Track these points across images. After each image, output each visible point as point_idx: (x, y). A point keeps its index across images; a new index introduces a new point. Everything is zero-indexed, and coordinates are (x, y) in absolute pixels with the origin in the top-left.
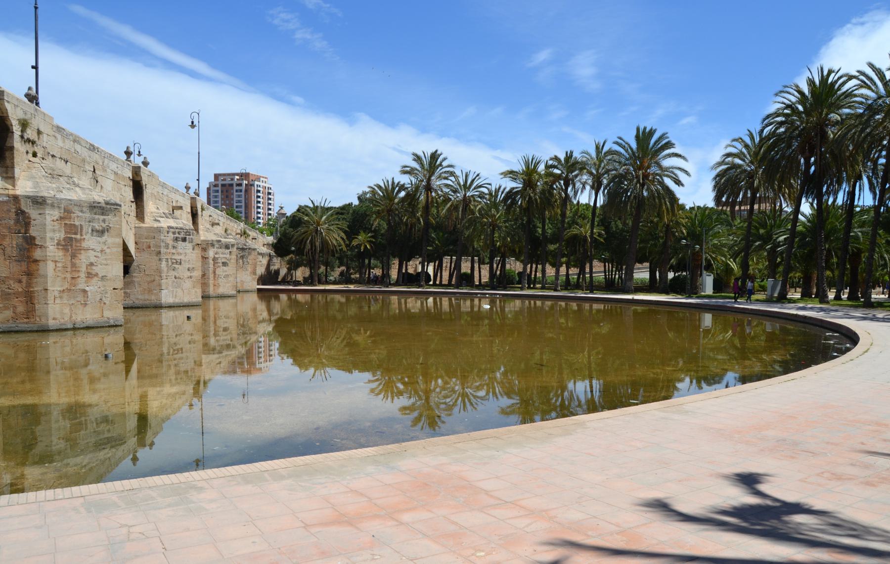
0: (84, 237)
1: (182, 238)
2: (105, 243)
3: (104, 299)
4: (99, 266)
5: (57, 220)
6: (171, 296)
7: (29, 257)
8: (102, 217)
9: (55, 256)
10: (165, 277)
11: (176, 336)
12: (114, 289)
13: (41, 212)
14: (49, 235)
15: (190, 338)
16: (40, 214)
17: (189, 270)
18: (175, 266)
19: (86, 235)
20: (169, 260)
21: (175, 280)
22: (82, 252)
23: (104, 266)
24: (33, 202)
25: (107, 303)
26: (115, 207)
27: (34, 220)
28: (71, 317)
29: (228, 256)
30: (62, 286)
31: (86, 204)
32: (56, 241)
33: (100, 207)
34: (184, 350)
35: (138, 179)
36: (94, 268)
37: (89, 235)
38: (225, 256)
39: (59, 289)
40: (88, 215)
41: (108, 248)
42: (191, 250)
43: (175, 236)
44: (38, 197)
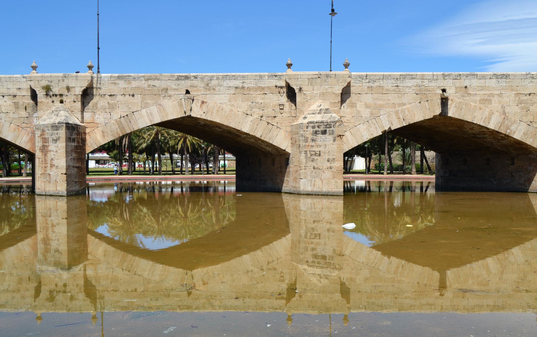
1: (322, 131)
3: (57, 179)
4: (56, 160)
6: (309, 184)
8: (56, 132)
10: (304, 168)
11: (314, 222)
12: (62, 174)
15: (328, 226)
17: (328, 161)
18: (313, 157)
20: (308, 152)
21: (314, 171)
22: (49, 152)
23: (57, 160)
26: (62, 125)
28: (44, 188)
30: (41, 171)
33: (56, 126)
34: (321, 236)
36: (53, 161)
37: (51, 143)
39: (41, 173)
40: (50, 132)
41: (59, 149)
42: (332, 142)
43: (315, 129)
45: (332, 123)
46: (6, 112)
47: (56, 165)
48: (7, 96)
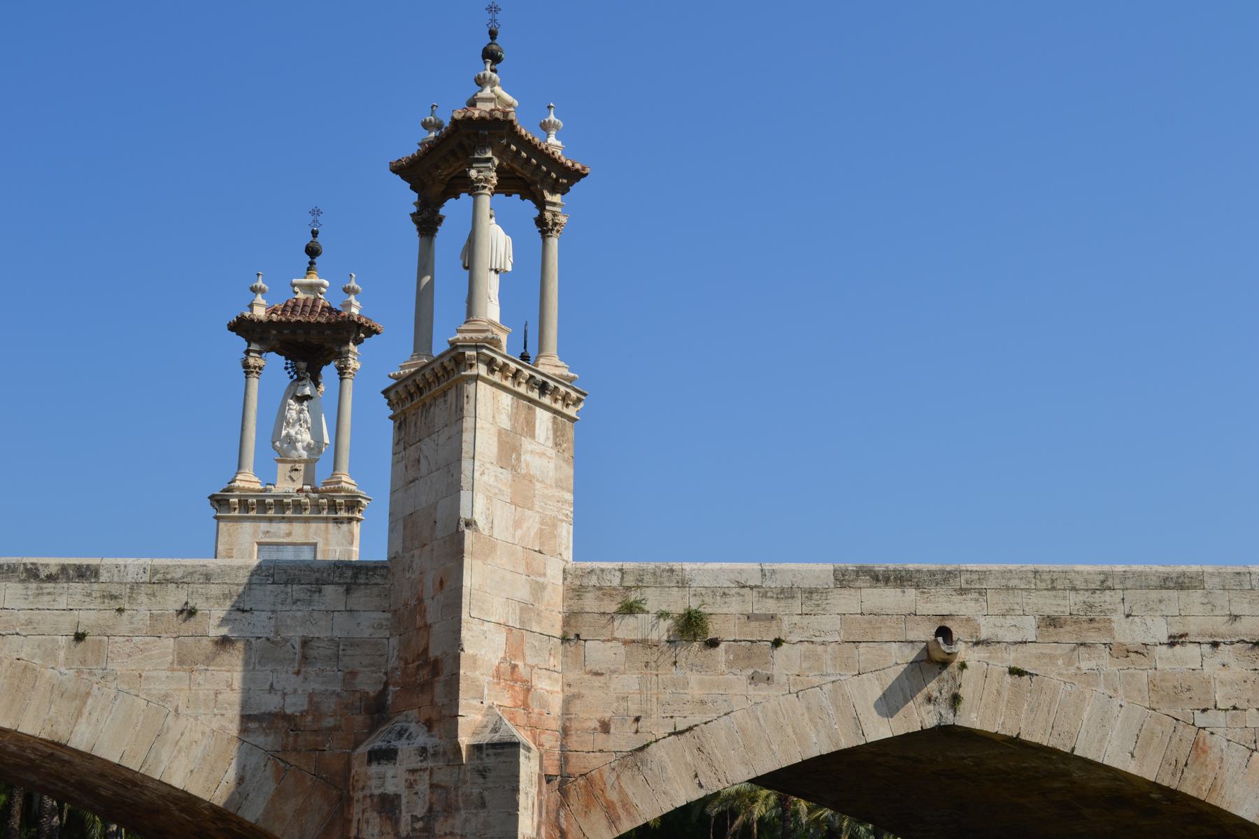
46: (1229, 705)
48: (1232, 643)
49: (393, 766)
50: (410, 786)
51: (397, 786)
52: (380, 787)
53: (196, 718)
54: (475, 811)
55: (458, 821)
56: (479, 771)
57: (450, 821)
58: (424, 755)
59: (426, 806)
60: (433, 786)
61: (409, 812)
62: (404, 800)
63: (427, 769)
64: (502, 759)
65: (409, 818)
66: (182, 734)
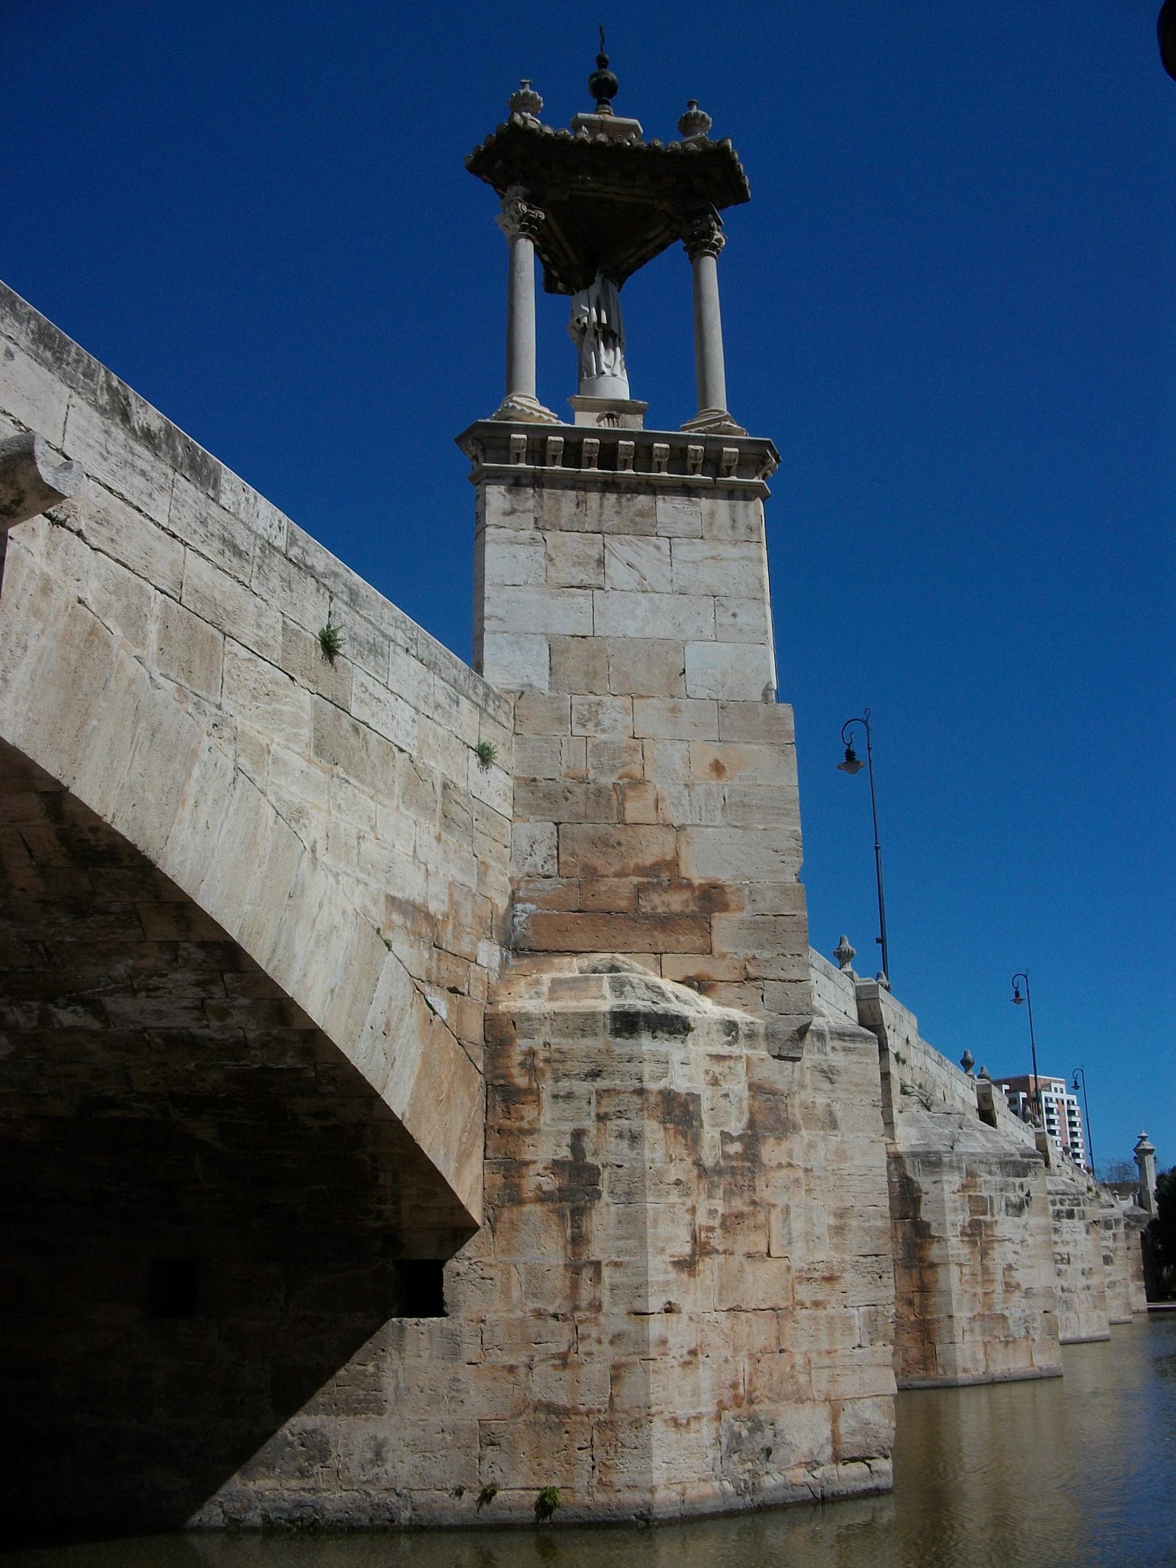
0: (996, 1217)
2: (1025, 1227)
3: (1031, 1332)
4: (1021, 1270)
5: (959, 1191)
7: (922, 1260)
8: (1018, 1181)
9: (959, 1255)
12: (1045, 1312)
13: (936, 1178)
14: (949, 1218)
16: (935, 1182)
19: (999, 1214)
22: (996, 1245)
23: (1028, 1270)
24: (923, 1162)
25: (1037, 1338)
27: (927, 1193)
28: (987, 1366)
29: (1110, 1243)
30: (972, 1310)
31: (995, 1159)
32: (959, 1229)
35: (986, 1107)
36: (1014, 1273)
37: (1003, 1214)
38: (1104, 1243)
40: (998, 1178)
43: (1056, 1208)
44: (929, 1153)
45: (1081, 1197)
47: (1024, 1287)
49: (680, 1045)
50: (715, 1082)
51: (690, 1080)
52: (660, 1078)
53: (336, 875)
54: (822, 1132)
55: (797, 1143)
56: (822, 1071)
57: (785, 1145)
58: (733, 1033)
59: (746, 1117)
60: (756, 1088)
61: (717, 1125)
62: (705, 1105)
63: (741, 1057)
64: (854, 1058)
65: (717, 1136)
66: (321, 906)
